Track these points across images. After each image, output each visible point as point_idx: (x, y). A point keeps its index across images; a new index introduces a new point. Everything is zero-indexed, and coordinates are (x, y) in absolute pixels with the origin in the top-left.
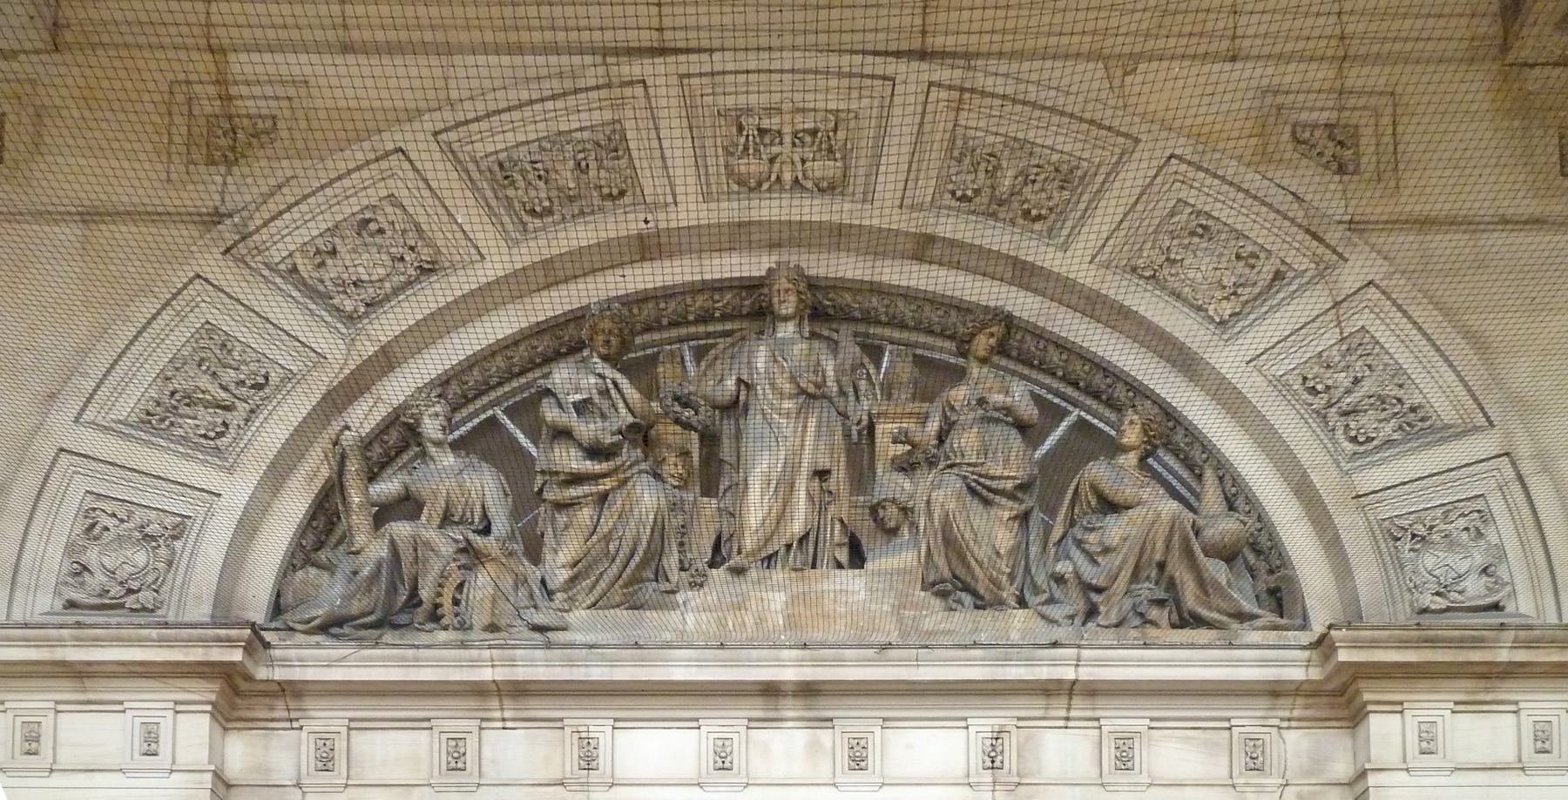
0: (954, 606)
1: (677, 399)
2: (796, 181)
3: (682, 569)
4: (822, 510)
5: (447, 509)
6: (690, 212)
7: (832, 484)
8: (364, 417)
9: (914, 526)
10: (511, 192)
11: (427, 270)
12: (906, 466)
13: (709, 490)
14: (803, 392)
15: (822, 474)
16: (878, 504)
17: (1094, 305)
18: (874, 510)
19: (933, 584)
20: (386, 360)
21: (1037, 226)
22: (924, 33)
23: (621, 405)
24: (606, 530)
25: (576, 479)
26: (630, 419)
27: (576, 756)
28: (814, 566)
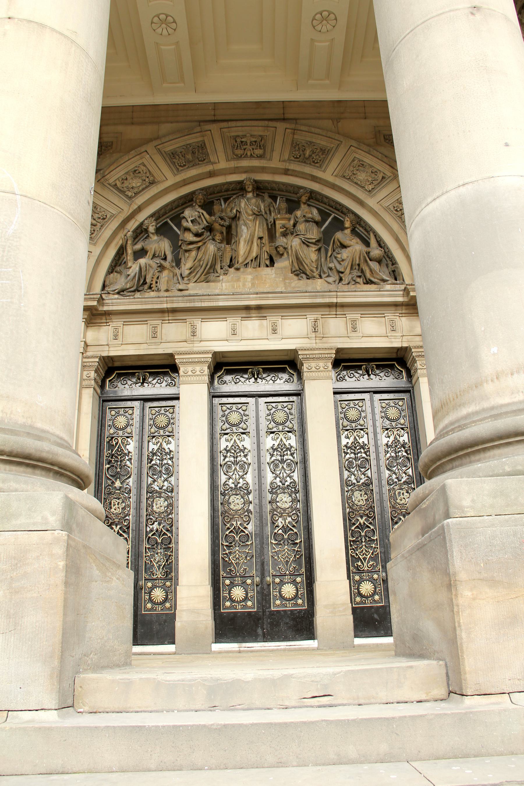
0: (301, 278)
1: (220, 217)
2: (251, 154)
3: (221, 269)
4: (261, 248)
5: (154, 253)
6: (223, 165)
7: (264, 241)
8: (132, 225)
9: (288, 252)
10: (174, 160)
11: (152, 183)
12: (284, 235)
13: (229, 243)
14: (254, 214)
15: (261, 238)
16: (277, 247)
17: (333, 187)
18: (276, 248)
19: (294, 271)
20: (139, 209)
21: (317, 165)
22: (284, 114)
23: (204, 220)
24: (200, 258)
25: (191, 243)
26: (207, 224)
27: (190, 332)
28: (259, 267)
